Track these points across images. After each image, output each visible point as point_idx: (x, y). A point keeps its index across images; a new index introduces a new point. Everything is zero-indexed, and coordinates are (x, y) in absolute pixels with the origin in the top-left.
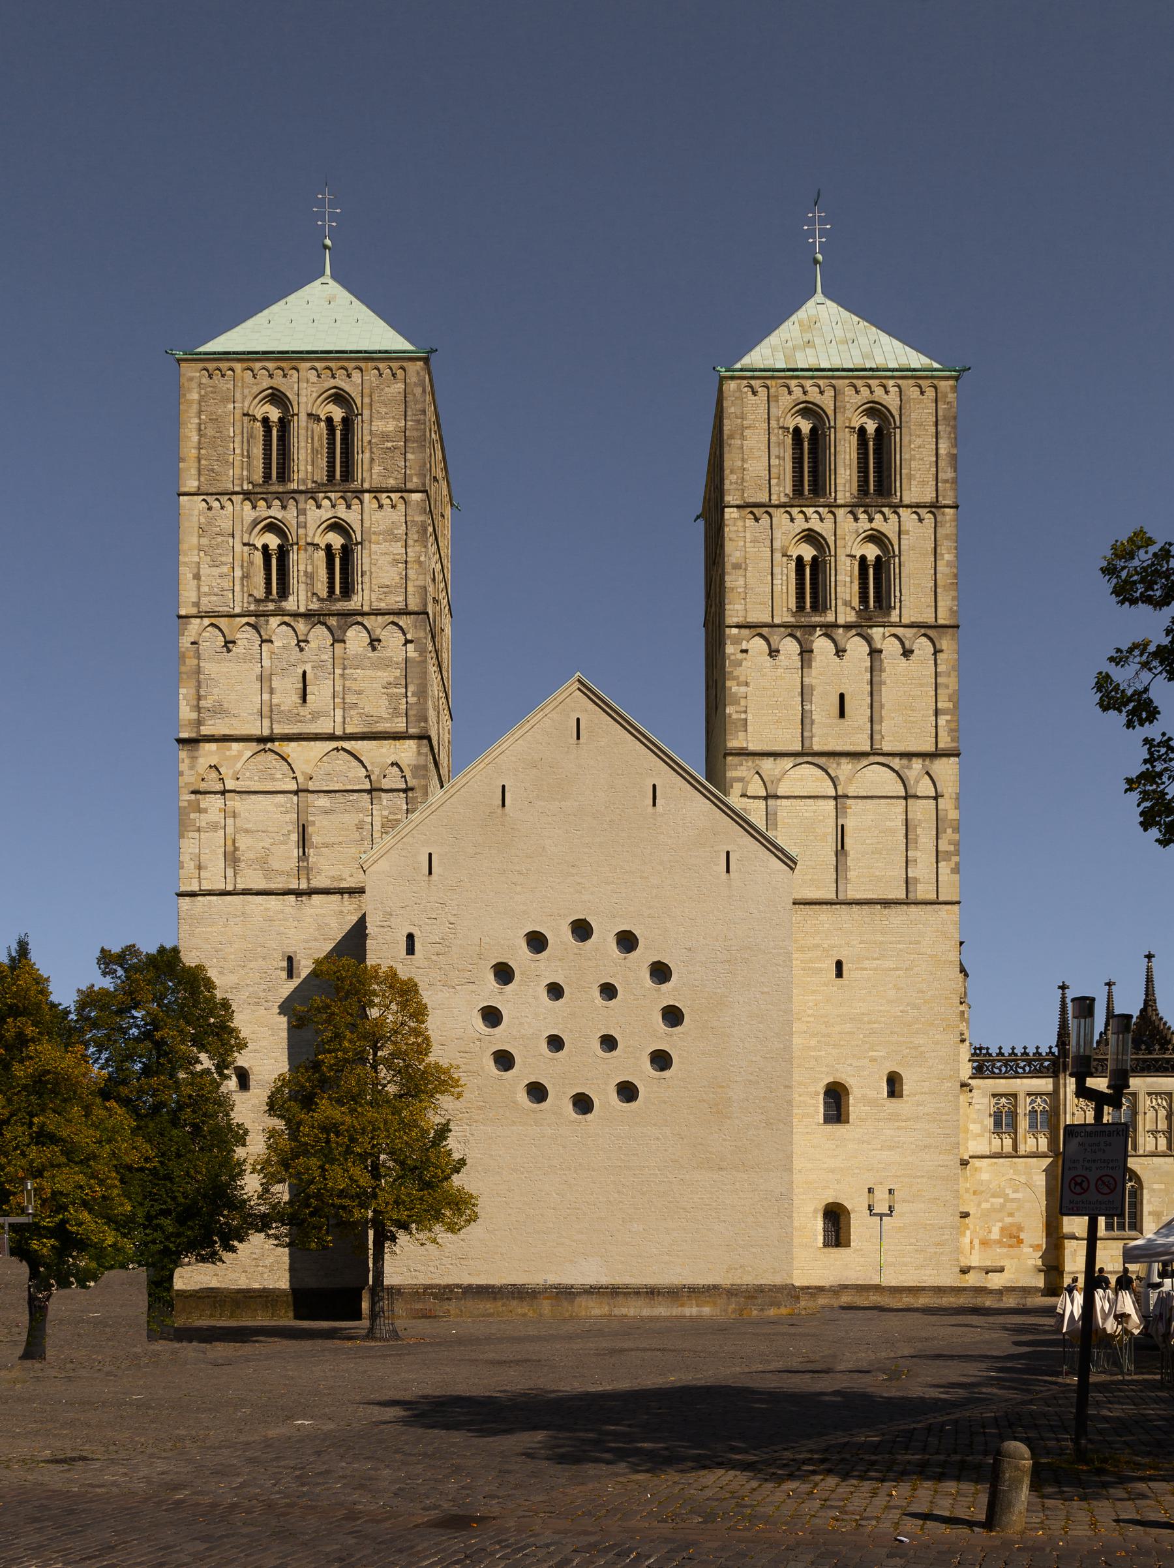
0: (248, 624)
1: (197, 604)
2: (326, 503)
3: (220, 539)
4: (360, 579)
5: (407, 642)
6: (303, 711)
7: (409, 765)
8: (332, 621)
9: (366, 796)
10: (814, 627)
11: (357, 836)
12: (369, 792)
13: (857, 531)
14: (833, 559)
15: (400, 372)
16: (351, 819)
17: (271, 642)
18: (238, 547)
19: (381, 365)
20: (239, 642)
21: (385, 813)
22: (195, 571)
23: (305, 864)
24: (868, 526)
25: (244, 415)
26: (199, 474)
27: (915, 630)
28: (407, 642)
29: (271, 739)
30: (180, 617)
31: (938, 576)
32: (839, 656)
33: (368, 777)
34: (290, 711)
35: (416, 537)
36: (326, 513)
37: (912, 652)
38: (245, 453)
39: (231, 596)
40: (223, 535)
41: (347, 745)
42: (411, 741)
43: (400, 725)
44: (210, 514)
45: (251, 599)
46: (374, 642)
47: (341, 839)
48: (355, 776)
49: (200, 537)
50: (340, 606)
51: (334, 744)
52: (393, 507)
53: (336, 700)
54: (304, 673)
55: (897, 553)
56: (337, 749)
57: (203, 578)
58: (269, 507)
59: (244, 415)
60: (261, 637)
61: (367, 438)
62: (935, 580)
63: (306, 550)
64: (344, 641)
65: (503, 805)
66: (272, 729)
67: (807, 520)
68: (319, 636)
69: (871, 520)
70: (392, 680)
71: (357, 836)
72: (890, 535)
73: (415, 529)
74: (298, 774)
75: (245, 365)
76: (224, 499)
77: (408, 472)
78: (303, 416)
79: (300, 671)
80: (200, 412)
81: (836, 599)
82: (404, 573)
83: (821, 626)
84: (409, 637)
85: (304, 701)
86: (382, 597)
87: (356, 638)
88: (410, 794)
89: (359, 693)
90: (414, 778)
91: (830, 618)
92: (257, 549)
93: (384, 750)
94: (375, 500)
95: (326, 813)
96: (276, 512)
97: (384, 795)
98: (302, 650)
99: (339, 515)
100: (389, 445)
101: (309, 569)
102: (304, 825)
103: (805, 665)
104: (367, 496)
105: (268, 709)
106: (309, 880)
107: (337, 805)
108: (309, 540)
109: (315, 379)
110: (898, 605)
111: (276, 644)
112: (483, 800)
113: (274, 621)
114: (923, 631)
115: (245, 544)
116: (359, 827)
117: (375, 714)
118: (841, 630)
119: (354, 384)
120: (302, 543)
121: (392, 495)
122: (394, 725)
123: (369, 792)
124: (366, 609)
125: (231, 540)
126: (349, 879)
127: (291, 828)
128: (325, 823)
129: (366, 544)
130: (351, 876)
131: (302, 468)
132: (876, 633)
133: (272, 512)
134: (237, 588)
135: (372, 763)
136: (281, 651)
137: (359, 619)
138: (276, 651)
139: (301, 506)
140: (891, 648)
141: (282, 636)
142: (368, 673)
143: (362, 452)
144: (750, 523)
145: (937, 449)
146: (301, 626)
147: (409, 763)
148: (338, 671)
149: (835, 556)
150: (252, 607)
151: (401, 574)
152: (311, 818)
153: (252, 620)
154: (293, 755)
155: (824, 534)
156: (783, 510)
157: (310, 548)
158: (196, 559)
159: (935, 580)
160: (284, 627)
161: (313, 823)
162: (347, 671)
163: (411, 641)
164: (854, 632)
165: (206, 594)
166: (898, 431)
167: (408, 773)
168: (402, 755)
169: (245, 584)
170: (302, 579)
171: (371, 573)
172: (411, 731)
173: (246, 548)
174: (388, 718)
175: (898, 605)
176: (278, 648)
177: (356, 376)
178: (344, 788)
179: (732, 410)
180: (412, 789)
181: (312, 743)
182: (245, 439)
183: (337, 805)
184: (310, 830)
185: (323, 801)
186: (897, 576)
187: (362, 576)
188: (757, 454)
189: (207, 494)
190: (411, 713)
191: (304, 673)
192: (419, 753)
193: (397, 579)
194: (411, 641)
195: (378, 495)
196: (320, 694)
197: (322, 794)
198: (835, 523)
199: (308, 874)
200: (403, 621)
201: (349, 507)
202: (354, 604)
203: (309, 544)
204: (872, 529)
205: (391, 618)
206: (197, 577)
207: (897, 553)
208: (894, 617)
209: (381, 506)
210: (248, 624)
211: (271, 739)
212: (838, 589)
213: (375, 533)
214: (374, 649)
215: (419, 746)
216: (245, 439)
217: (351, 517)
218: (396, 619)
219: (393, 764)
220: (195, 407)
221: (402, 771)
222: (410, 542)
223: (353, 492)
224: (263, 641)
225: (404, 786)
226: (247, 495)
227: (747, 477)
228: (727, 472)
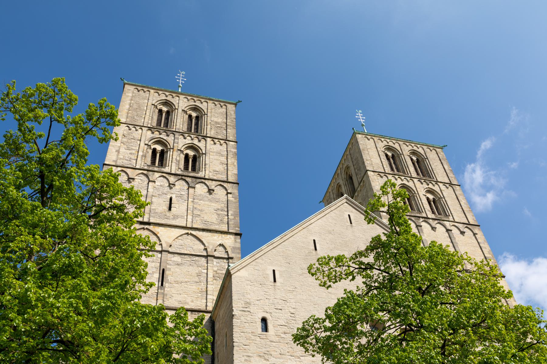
0: (142, 173)
1: (116, 161)
2: (189, 138)
3: (133, 140)
4: (204, 167)
5: (228, 193)
6: (168, 214)
7: (230, 247)
8: (188, 179)
9: (203, 259)
10: (419, 217)
11: (197, 279)
12: (207, 257)
13: (423, 187)
14: (417, 195)
15: (224, 107)
16: (194, 270)
17: (154, 182)
18: (142, 144)
19: (216, 103)
20: (136, 180)
21: (215, 269)
22: (118, 149)
23: (162, 291)
24: (427, 187)
25: (152, 105)
26: (127, 118)
27: (462, 225)
28: (228, 193)
29: (149, 224)
30: (104, 164)
31: (463, 207)
32: (434, 230)
33: (206, 249)
34: (161, 213)
35: (232, 156)
36: (188, 141)
37: (464, 232)
38: (151, 116)
39: (135, 161)
40: (134, 139)
41: (194, 232)
42: (231, 236)
43: (224, 228)
44: (129, 131)
45: (145, 165)
46: (210, 191)
47: (186, 280)
48: (198, 248)
49: (122, 138)
50: (192, 174)
51: (186, 231)
52: (221, 145)
53: (188, 211)
54: (171, 199)
55: (442, 197)
56: (188, 234)
57: (121, 153)
58: (160, 134)
59: (152, 105)
60: (149, 179)
61: (209, 121)
62: (462, 209)
63: (177, 151)
64: (194, 188)
65: (316, 249)
66: (149, 220)
67: (402, 180)
68: (181, 185)
69: (428, 185)
70: (220, 208)
71: (197, 279)
72: (437, 191)
73: (231, 153)
74: (163, 242)
75: (155, 91)
76: (138, 128)
77: (228, 135)
78: (180, 110)
79: (169, 197)
80: (131, 100)
81: (424, 209)
82: (226, 168)
83: (422, 217)
84: (229, 191)
85: (170, 209)
86: (215, 175)
87: (201, 189)
88: (230, 261)
89: (201, 211)
90: (233, 253)
91: (424, 215)
92: (151, 148)
93: (215, 238)
94: (212, 141)
95: (178, 265)
96: (163, 136)
97: (215, 260)
98: (171, 188)
99: (195, 143)
100: (219, 126)
101: (178, 159)
102: (163, 270)
103: (420, 231)
104: (208, 139)
105: (149, 210)
106: (163, 301)
107: (185, 262)
108: (179, 149)
109: (187, 101)
110: (451, 215)
111: (157, 183)
112: (303, 245)
113: (157, 175)
114: (466, 225)
115: (146, 144)
116: (199, 275)
117: (210, 221)
118: (431, 220)
119: (204, 106)
120: (175, 148)
121: (221, 141)
122: (221, 227)
123: (207, 257)
124: (206, 177)
125: (139, 142)
126: (190, 303)
127: (154, 270)
128: (177, 270)
129: (208, 155)
130: (192, 302)
131: (178, 124)
132: (447, 224)
133: (161, 136)
134: (139, 159)
135: (208, 243)
136: (159, 187)
137: (203, 181)
138: (157, 187)
139: (176, 136)
140: (455, 231)
141: (161, 182)
142: (206, 203)
143: (207, 125)
144: (379, 178)
145: (444, 167)
146: (172, 179)
147: (231, 245)
148: (190, 200)
149: (418, 194)
150: (146, 168)
151: (224, 168)
152: (168, 266)
153: (145, 172)
154: (160, 233)
155: (411, 186)
156: (392, 176)
157: (179, 152)
158: (119, 145)
159: (462, 209)
160: (162, 178)
161: (170, 269)
162: (195, 201)
163: (231, 193)
164: (436, 222)
165: (121, 159)
166: (427, 160)
167: (229, 250)
168: (226, 241)
169: (143, 158)
170: (174, 161)
171: (210, 165)
172: (230, 231)
173: (146, 146)
174: (217, 224)
175: (451, 215)
176: (157, 185)
177: (205, 104)
178: (190, 253)
179: (362, 142)
180: (232, 258)
181: (173, 229)
182: (151, 112)
183: (185, 262)
184: (167, 273)
185: (177, 258)
186: (446, 205)
187: (205, 165)
188: (375, 157)
189: (130, 124)
190: (230, 223)
191: (171, 199)
192: (236, 242)
193: (223, 170)
194: (231, 193)
195: (214, 139)
196: (179, 208)
197: (177, 255)
198: (414, 183)
199: (163, 297)
200: (225, 185)
201: (199, 141)
202: (201, 174)
203: (179, 150)
204: (429, 188)
205: (220, 183)
206: (118, 151)
207: (442, 197)
208: (451, 218)
209: (215, 144)
210: (142, 173)
211: (149, 224)
212: (424, 205)
213: (212, 152)
214: (210, 194)
215: (235, 238)
216: (151, 112)
217: (201, 145)
218: (222, 183)
219: (220, 245)
220: (129, 98)
221: (225, 248)
222: (229, 157)
223: (202, 136)
224: (149, 181)
225: (226, 256)
226: (150, 129)
227: (373, 163)
228: (365, 160)
